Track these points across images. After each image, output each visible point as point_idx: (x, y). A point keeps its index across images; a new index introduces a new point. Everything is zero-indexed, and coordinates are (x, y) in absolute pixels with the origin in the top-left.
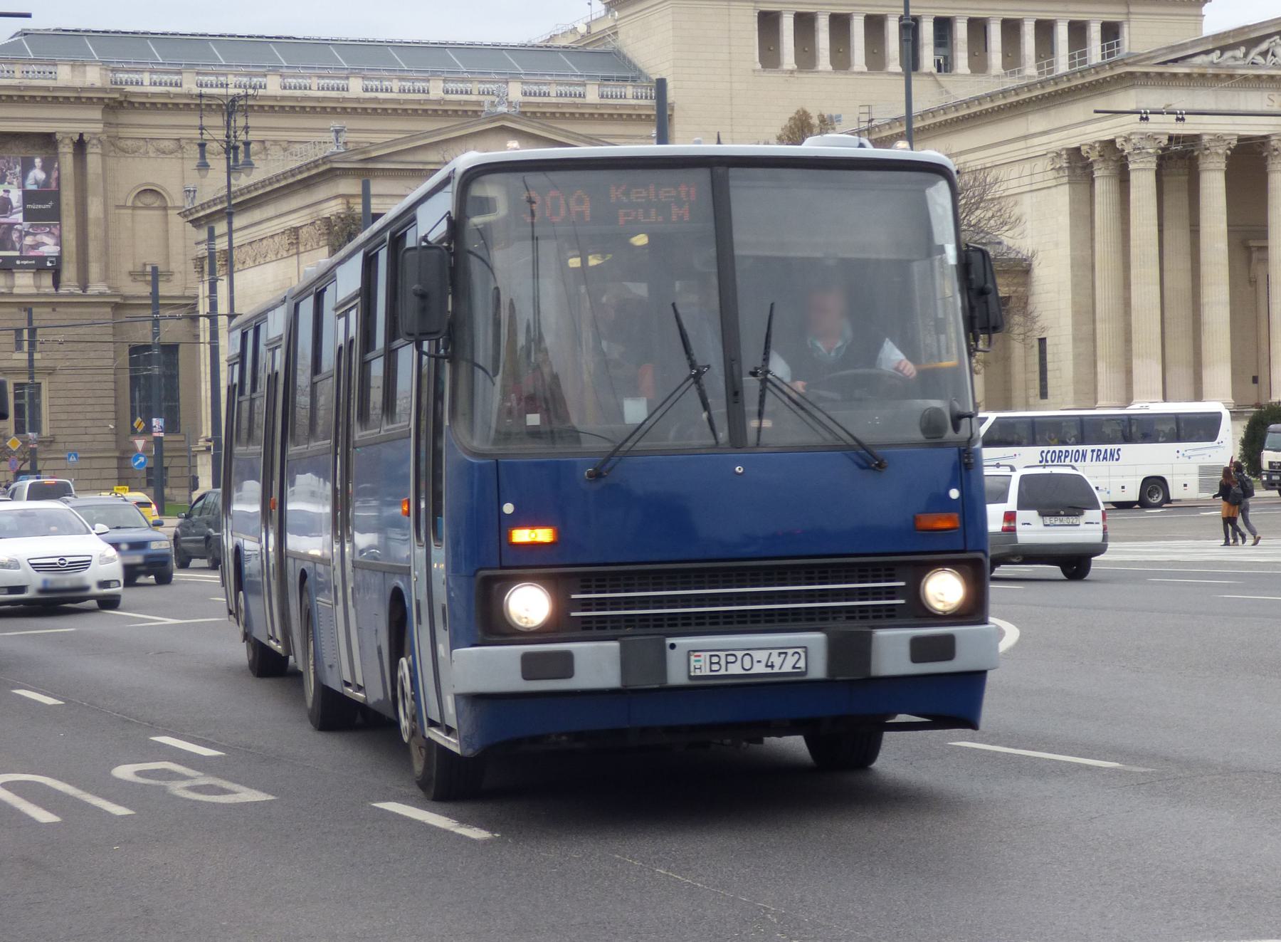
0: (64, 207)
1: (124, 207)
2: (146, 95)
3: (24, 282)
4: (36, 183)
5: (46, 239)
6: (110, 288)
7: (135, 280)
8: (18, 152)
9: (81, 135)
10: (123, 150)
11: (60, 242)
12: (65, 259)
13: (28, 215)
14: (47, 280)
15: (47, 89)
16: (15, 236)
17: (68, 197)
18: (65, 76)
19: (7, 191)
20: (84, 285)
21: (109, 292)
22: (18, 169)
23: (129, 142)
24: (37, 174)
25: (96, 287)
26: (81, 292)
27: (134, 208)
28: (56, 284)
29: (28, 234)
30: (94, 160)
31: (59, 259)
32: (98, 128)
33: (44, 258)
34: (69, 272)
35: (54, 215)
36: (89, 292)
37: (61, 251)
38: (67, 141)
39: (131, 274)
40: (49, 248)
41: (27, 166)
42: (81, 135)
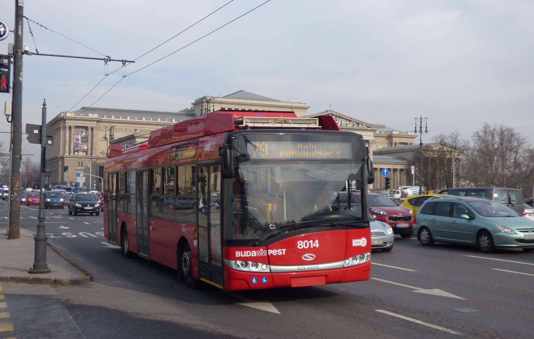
0: (88, 140)
1: (100, 140)
2: (105, 120)
3: (81, 154)
4: (84, 135)
5: (85, 146)
6: (96, 155)
7: (101, 154)
8: (81, 130)
9: (92, 127)
10: (100, 130)
11: (87, 147)
12: (88, 149)
13: (82, 141)
14: (85, 153)
15: (87, 118)
16: (79, 145)
17: (90, 138)
18: (90, 116)
19: (78, 137)
20: (92, 154)
21: (96, 156)
22: (80, 133)
23: (101, 128)
24: (84, 134)
25: (94, 155)
26: (91, 156)
27: (101, 141)
28: (87, 154)
29: (82, 145)
30: (95, 132)
31: (87, 150)
32: (95, 126)
33: (84, 149)
34: (89, 152)
35: (87, 141)
36: (92, 156)
37: (88, 148)
38: (90, 128)
39: (100, 153)
40: (85, 148)
41: (82, 132)
42: (92, 127)
